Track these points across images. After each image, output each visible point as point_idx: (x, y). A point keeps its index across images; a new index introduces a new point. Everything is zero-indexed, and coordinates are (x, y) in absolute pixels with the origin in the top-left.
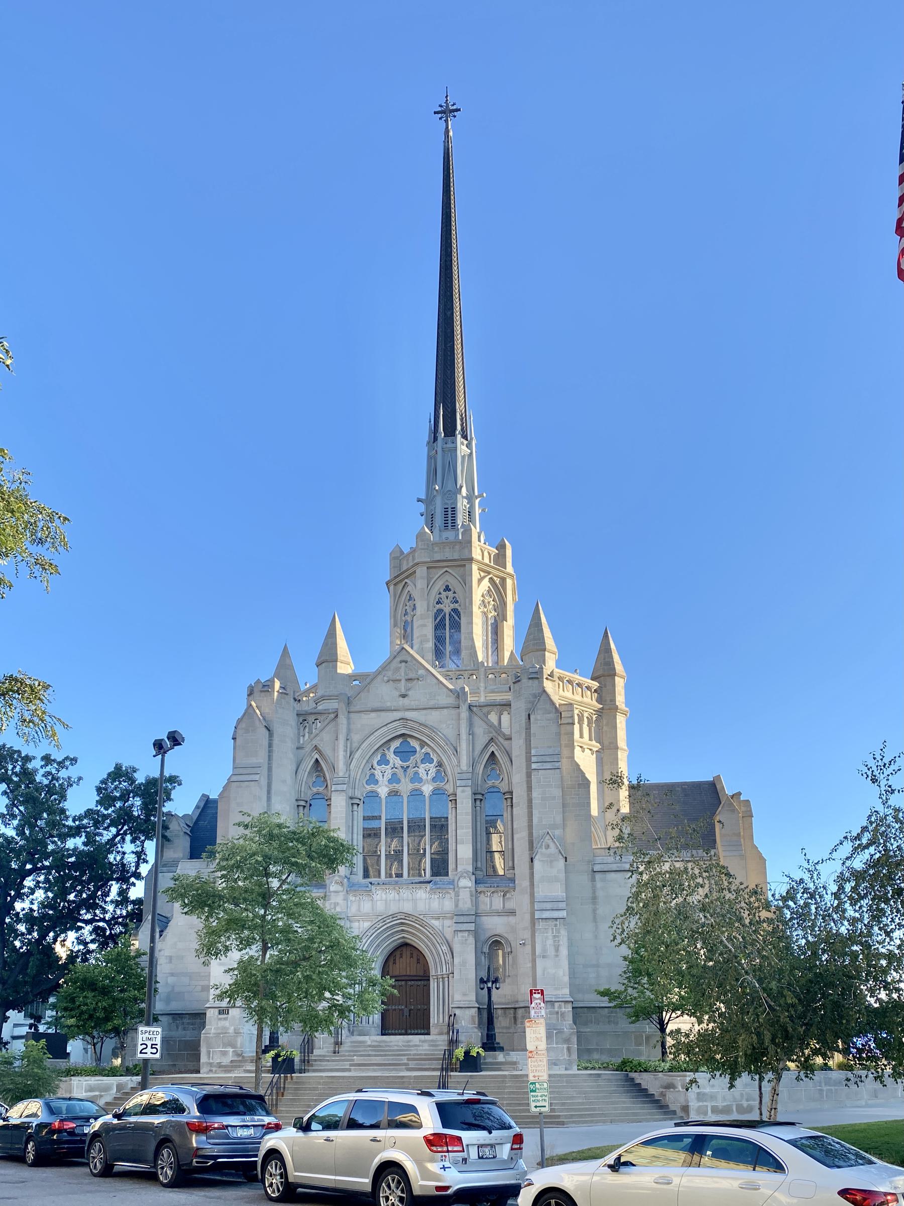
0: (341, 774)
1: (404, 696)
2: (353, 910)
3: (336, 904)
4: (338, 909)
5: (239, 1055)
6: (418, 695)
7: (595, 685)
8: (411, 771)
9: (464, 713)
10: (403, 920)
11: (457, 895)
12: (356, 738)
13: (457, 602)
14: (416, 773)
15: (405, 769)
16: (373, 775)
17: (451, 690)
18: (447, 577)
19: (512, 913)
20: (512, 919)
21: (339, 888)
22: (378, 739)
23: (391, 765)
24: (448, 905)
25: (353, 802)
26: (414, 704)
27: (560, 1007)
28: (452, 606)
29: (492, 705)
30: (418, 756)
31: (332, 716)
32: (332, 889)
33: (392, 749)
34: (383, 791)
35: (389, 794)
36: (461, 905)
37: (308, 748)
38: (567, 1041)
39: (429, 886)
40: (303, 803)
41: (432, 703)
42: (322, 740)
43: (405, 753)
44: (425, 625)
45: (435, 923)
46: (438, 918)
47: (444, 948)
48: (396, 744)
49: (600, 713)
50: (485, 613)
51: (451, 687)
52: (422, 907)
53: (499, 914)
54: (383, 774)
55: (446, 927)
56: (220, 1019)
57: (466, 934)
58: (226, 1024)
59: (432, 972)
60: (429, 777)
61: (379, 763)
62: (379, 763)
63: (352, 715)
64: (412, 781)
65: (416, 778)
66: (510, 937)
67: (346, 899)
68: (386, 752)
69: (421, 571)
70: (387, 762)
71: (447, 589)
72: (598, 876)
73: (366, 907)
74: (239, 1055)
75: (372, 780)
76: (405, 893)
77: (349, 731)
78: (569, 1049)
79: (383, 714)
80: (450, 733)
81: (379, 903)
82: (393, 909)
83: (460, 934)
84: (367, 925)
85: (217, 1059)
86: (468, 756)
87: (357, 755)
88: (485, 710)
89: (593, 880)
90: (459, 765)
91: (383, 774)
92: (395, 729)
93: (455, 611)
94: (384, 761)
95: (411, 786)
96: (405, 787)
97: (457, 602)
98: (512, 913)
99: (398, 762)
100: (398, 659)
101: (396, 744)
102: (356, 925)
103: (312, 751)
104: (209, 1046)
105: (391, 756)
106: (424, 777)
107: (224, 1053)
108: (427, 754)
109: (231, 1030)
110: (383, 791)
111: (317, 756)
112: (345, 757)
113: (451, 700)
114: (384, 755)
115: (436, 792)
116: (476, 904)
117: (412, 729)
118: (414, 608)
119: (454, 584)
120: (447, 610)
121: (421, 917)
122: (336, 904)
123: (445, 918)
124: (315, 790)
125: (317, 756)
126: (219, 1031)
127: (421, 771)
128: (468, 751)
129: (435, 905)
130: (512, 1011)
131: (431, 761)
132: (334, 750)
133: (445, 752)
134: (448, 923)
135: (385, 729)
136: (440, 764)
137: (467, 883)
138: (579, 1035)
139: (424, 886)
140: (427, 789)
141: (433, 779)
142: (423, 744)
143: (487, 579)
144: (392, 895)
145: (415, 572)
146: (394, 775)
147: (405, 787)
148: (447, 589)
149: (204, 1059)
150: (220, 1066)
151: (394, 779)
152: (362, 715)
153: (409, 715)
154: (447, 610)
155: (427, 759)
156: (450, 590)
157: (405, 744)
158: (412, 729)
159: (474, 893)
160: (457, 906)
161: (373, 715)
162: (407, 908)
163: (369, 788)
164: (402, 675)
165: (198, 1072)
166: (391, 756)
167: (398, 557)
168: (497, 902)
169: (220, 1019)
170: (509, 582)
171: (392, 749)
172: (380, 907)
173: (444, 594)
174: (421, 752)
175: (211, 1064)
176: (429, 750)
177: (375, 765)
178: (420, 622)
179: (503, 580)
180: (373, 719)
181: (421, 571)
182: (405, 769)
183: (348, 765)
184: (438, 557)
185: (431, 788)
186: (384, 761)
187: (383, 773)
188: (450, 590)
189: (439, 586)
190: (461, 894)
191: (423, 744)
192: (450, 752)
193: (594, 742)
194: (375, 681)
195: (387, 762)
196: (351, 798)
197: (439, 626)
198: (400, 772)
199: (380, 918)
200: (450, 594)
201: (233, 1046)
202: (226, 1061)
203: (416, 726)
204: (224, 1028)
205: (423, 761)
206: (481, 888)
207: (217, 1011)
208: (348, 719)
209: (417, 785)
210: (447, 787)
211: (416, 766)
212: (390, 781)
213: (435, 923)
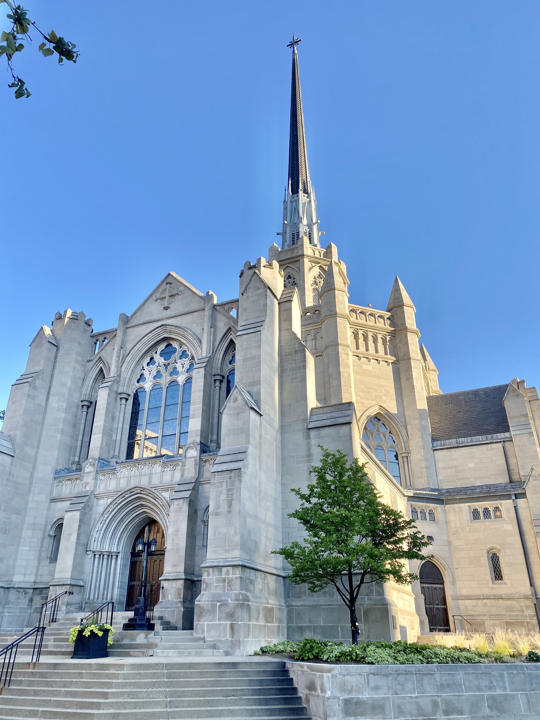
7: (388, 314)
8: (170, 368)
12: (129, 346)
14: (176, 368)
30: (177, 355)
32: (87, 470)
33: (159, 352)
34: (148, 385)
36: (186, 475)
40: (85, 403)
48: (162, 346)
49: (393, 334)
54: (149, 373)
62: (148, 364)
65: (175, 372)
67: (96, 479)
68: (154, 354)
81: (122, 480)
83: (176, 502)
87: (128, 359)
91: (149, 373)
95: (169, 379)
101: (162, 346)
102: (101, 502)
105: (158, 358)
108: (185, 351)
110: (148, 385)
112: (117, 362)
117: (171, 332)
121: (152, 490)
125: (101, 365)
127: (179, 366)
129: (167, 478)
146: (159, 372)
147: (165, 380)
151: (158, 375)
155: (184, 355)
157: (166, 345)
159: (198, 461)
160: (182, 476)
162: (144, 483)
166: (158, 358)
171: (159, 352)
177: (146, 367)
185: (184, 377)
190: (187, 464)
191: (181, 344)
193: (389, 356)
198: (162, 369)
199: (120, 493)
200: (291, 280)
205: (181, 358)
206: (205, 456)
212: (155, 378)
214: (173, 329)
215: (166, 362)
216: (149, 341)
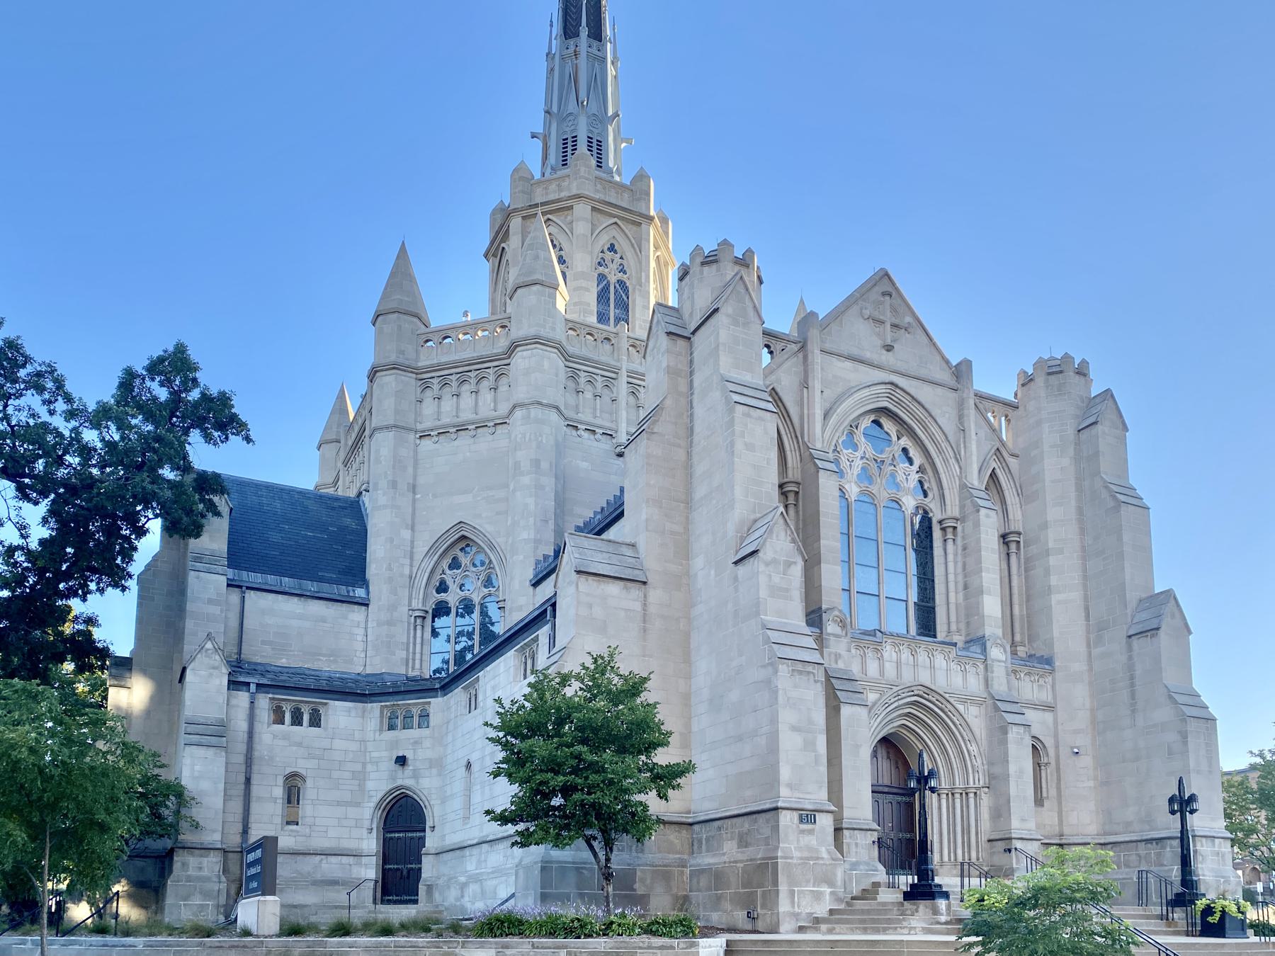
13: (625, 273)
18: (614, 232)
44: (587, 290)
56: (803, 832)
58: (812, 841)
71: (612, 248)
93: (621, 282)
96: (882, 491)
97: (625, 273)
104: (792, 882)
107: (817, 896)
119: (622, 245)
120: (613, 279)
126: (806, 854)
133: (940, 451)
135: (866, 392)
136: (921, 470)
145: (571, 208)
148: (612, 248)
156: (616, 252)
161: (848, 364)
169: (803, 832)
173: (609, 255)
175: (796, 916)
181: (582, 209)
183: (823, 433)
188: (616, 252)
189: (604, 240)
201: (831, 884)
202: (821, 910)
203: (906, 400)
207: (796, 815)
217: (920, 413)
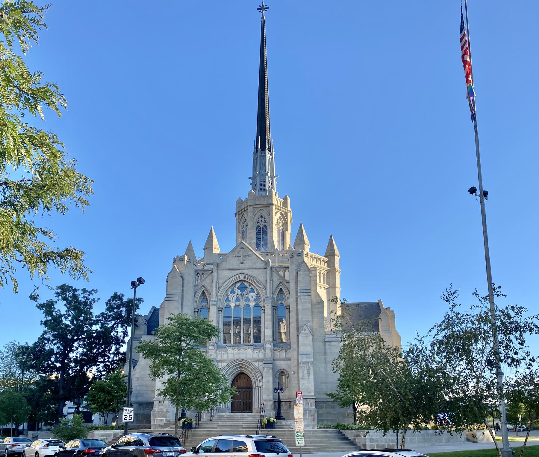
0: (214, 297)
1: (242, 263)
2: (219, 358)
3: (211, 355)
4: (212, 357)
5: (168, 421)
6: (248, 263)
7: (326, 259)
8: (245, 296)
9: (269, 272)
10: (241, 362)
11: (265, 351)
12: (221, 281)
14: (247, 297)
15: (242, 295)
16: (228, 298)
17: (263, 261)
18: (261, 211)
19: (289, 359)
20: (289, 362)
21: (213, 348)
22: (229, 283)
23: (236, 293)
24: (261, 356)
25: (219, 310)
26: (247, 267)
27: (310, 401)
28: (264, 224)
29: (281, 267)
30: (248, 290)
31: (210, 272)
32: (210, 348)
33: (237, 287)
34: (233, 305)
35: (235, 307)
36: (266, 356)
37: (200, 286)
38: (313, 416)
39: (252, 347)
40: (197, 310)
41: (254, 266)
42: (206, 282)
43: (242, 288)
45: (255, 363)
46: (256, 362)
47: (259, 375)
48: (238, 284)
49: (328, 271)
50: (278, 228)
51: (263, 259)
52: (249, 356)
53: (283, 359)
54: (233, 297)
55: (260, 365)
57: (269, 368)
58: (162, 407)
59: (254, 385)
60: (253, 299)
61: (231, 293)
62: (231, 293)
63: (219, 272)
64: (245, 300)
65: (247, 299)
66: (288, 370)
67: (216, 353)
69: (250, 209)
70: (234, 293)
71: (262, 217)
72: (327, 343)
73: (225, 356)
74: (168, 421)
75: (228, 300)
76: (242, 350)
77: (218, 278)
78: (314, 419)
79: (233, 271)
80: (262, 279)
82: (237, 357)
83: (266, 369)
84: (225, 364)
85: (158, 423)
86: (270, 290)
87: (221, 289)
88: (278, 270)
89: (325, 345)
90: (266, 294)
91: (233, 297)
92: (238, 278)
93: (265, 226)
94: (233, 292)
95: (245, 303)
96: (242, 303)
98: (289, 359)
99: (239, 292)
100: (239, 247)
101: (239, 284)
102: (220, 364)
103: (201, 287)
104: (155, 417)
105: (236, 290)
106: (251, 299)
107: (162, 420)
109: (165, 410)
110: (233, 305)
111: (203, 289)
113: (263, 265)
114: (233, 289)
115: (256, 306)
116: (273, 355)
117: (245, 278)
118: (247, 225)
119: (264, 215)
120: (261, 226)
122: (211, 355)
123: (259, 361)
124: (202, 304)
125: (203, 289)
127: (250, 296)
128: (270, 287)
130: (289, 403)
131: (254, 292)
132: (211, 287)
133: (260, 288)
134: (260, 363)
136: (258, 293)
137: (269, 346)
138: (318, 413)
139: (250, 347)
140: (252, 304)
141: (255, 300)
142: (250, 284)
143: (279, 213)
144: (236, 351)
146: (237, 298)
147: (242, 303)
148: (262, 217)
149: (152, 423)
150: (159, 426)
151: (238, 300)
152: (224, 272)
153: (244, 271)
154: (261, 226)
155: (252, 291)
157: (242, 284)
158: (245, 278)
160: (265, 356)
161: (229, 271)
162: (243, 357)
163: (226, 304)
164: (241, 254)
165: (150, 428)
166: (236, 290)
167: (240, 202)
168: (283, 354)
170: (289, 214)
171: (237, 287)
172: (231, 356)
174: (249, 288)
175: (155, 425)
176: (253, 287)
178: (250, 231)
179: (286, 213)
180: (228, 274)
182: (242, 295)
183: (217, 294)
184: (257, 203)
186: (233, 292)
187: (233, 297)
189: (258, 215)
191: (250, 284)
192: (262, 288)
193: (326, 285)
194: (230, 257)
195: (234, 293)
196: (219, 308)
197: (258, 233)
198: (240, 297)
200: (263, 219)
201: (165, 417)
202: (162, 423)
203: (247, 276)
204: (161, 409)
205: (250, 292)
208: (218, 273)
209: (247, 303)
210: (261, 303)
211: (247, 294)
213: (255, 363)
214: (247, 276)
215: (242, 293)
216: (232, 280)
217: (252, 279)
